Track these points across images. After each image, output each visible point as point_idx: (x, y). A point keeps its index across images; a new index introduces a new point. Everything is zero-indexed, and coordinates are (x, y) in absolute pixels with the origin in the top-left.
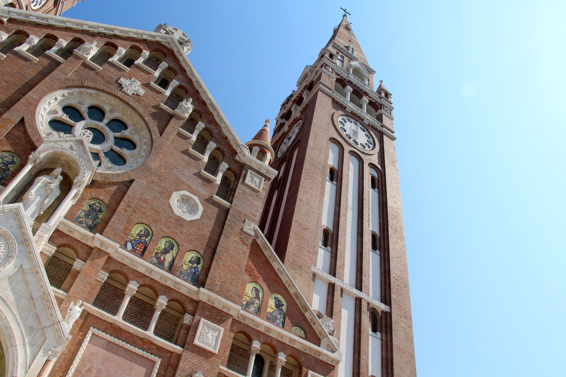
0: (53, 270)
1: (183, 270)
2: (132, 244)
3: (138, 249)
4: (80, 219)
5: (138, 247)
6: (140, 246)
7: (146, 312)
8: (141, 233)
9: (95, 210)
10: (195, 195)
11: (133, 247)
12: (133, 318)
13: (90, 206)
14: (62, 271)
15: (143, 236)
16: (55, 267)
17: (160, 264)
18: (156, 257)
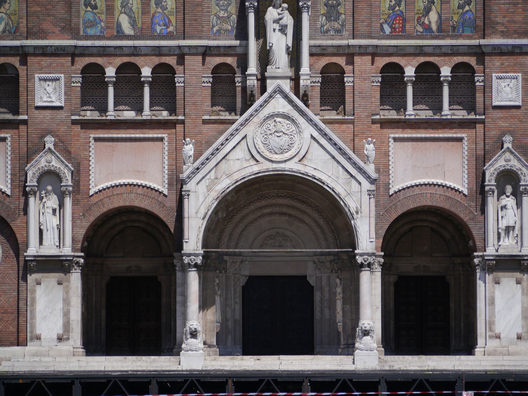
0: (328, 89)
1: (455, 23)
2: (388, 25)
3: (397, 25)
4: (325, 27)
5: (396, 23)
6: (397, 22)
7: (435, 84)
8: (392, 4)
9: (334, 7)
11: (391, 27)
13: (326, 5)
14: (336, 85)
15: (396, 7)
16: (328, 85)
18: (420, 25)
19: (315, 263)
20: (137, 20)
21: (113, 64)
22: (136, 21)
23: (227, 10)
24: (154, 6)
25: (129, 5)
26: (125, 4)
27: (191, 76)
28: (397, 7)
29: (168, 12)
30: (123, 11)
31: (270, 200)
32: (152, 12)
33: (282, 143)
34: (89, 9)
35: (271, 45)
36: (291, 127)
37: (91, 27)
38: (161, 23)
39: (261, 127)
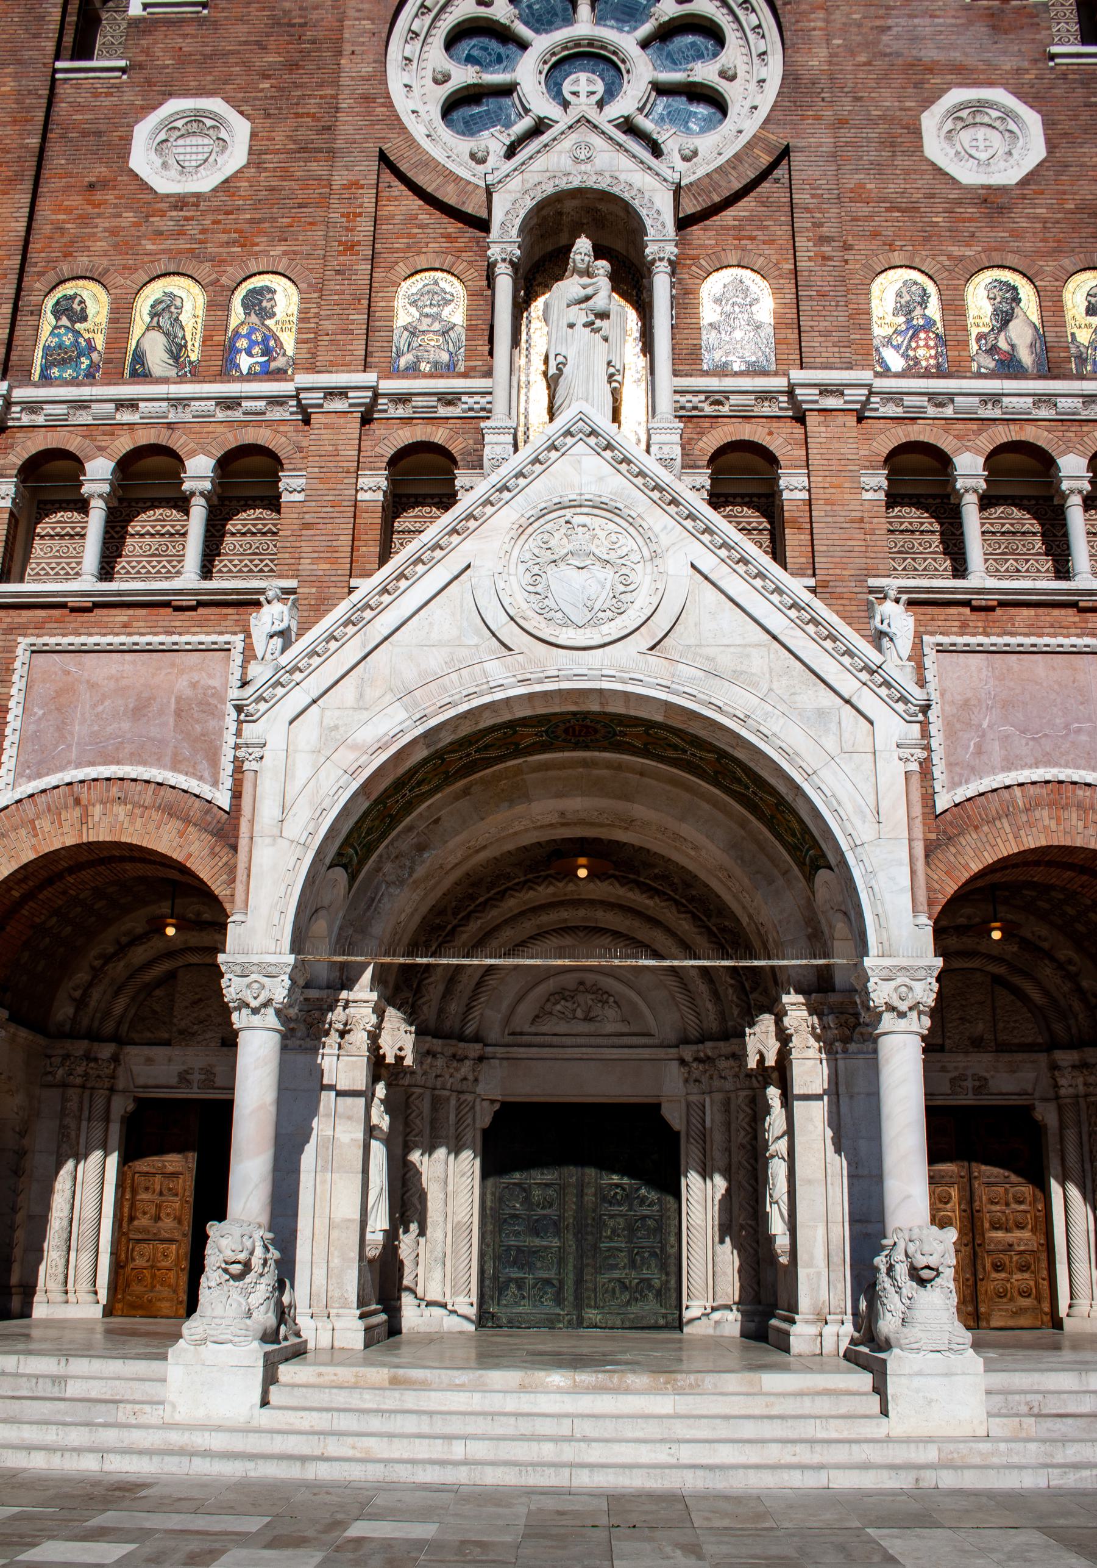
1: (1083, 349)
2: (897, 348)
5: (918, 347)
8: (903, 301)
10: (991, 84)
11: (905, 356)
12: (1007, 560)
17: (1009, 367)
18: (986, 352)
19: (682, 1062)
20: (189, 344)
21: (108, 450)
22: (186, 346)
23: (439, 315)
24: (241, 310)
25: (173, 309)
26: (163, 306)
27: (324, 470)
28: (918, 308)
29: (277, 323)
30: (154, 323)
31: (560, 885)
32: (233, 323)
33: (593, 589)
34: (64, 321)
35: (560, 359)
36: (622, 541)
37: (63, 363)
38: (256, 350)
39: (521, 542)
